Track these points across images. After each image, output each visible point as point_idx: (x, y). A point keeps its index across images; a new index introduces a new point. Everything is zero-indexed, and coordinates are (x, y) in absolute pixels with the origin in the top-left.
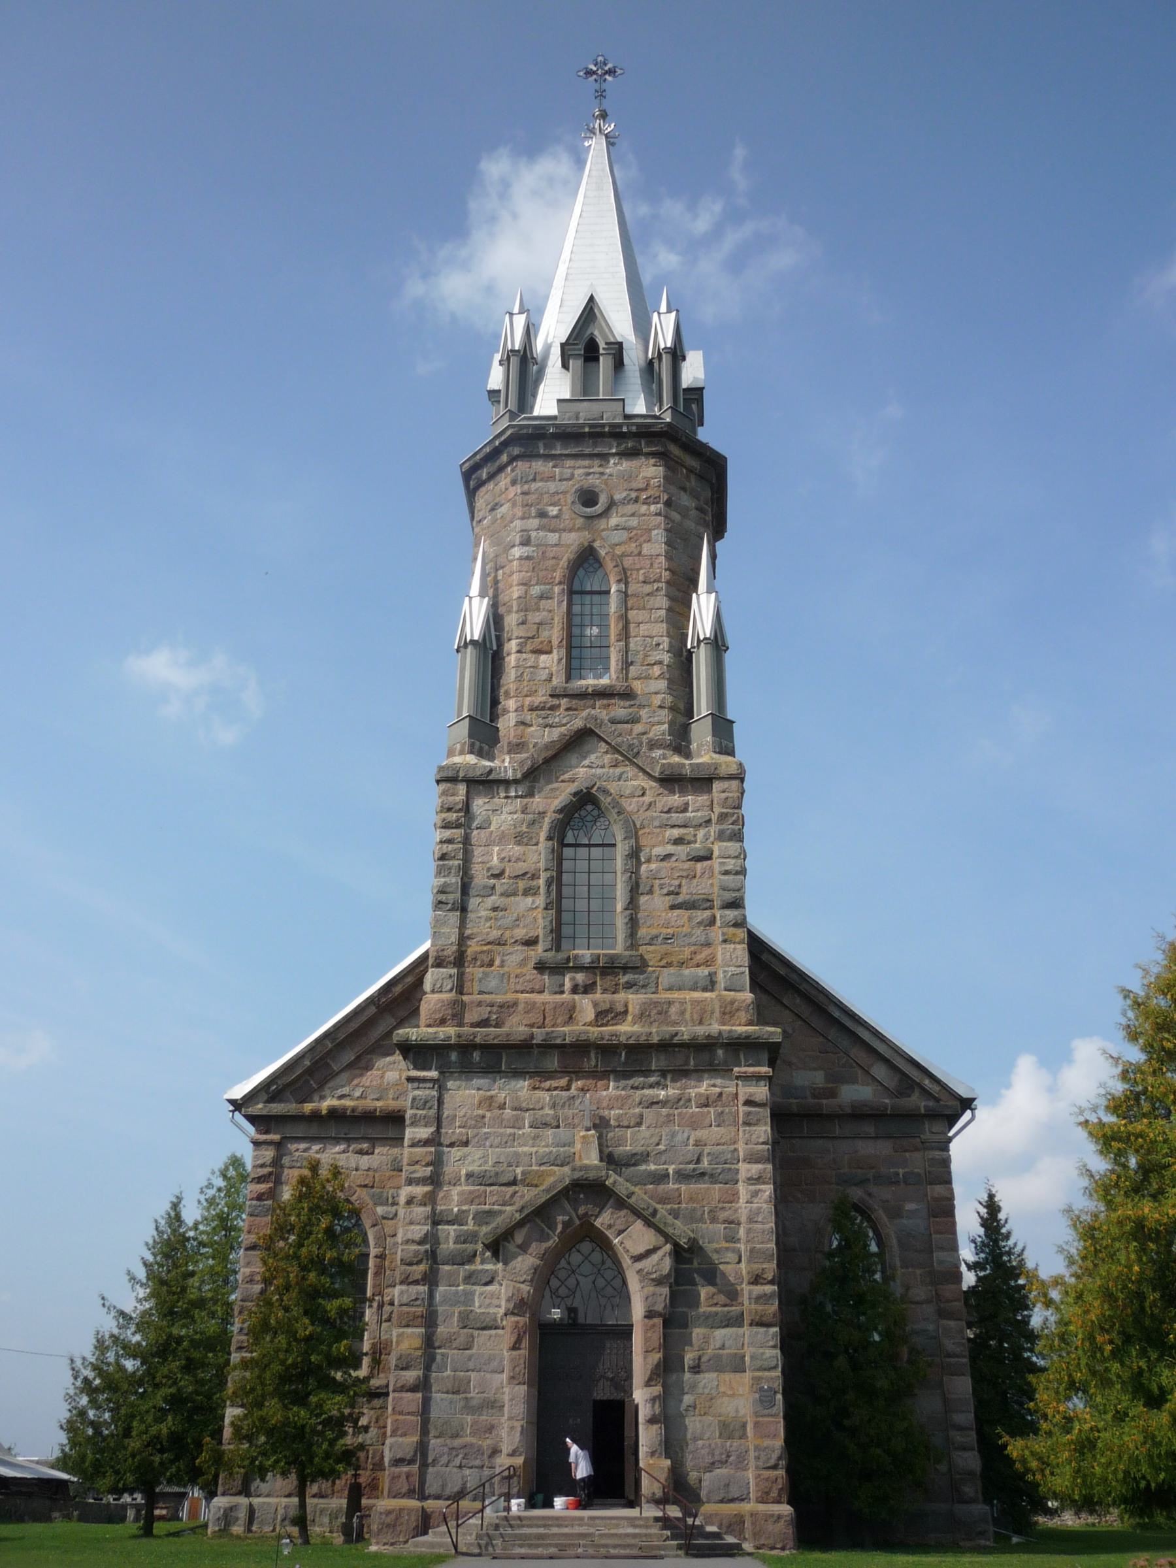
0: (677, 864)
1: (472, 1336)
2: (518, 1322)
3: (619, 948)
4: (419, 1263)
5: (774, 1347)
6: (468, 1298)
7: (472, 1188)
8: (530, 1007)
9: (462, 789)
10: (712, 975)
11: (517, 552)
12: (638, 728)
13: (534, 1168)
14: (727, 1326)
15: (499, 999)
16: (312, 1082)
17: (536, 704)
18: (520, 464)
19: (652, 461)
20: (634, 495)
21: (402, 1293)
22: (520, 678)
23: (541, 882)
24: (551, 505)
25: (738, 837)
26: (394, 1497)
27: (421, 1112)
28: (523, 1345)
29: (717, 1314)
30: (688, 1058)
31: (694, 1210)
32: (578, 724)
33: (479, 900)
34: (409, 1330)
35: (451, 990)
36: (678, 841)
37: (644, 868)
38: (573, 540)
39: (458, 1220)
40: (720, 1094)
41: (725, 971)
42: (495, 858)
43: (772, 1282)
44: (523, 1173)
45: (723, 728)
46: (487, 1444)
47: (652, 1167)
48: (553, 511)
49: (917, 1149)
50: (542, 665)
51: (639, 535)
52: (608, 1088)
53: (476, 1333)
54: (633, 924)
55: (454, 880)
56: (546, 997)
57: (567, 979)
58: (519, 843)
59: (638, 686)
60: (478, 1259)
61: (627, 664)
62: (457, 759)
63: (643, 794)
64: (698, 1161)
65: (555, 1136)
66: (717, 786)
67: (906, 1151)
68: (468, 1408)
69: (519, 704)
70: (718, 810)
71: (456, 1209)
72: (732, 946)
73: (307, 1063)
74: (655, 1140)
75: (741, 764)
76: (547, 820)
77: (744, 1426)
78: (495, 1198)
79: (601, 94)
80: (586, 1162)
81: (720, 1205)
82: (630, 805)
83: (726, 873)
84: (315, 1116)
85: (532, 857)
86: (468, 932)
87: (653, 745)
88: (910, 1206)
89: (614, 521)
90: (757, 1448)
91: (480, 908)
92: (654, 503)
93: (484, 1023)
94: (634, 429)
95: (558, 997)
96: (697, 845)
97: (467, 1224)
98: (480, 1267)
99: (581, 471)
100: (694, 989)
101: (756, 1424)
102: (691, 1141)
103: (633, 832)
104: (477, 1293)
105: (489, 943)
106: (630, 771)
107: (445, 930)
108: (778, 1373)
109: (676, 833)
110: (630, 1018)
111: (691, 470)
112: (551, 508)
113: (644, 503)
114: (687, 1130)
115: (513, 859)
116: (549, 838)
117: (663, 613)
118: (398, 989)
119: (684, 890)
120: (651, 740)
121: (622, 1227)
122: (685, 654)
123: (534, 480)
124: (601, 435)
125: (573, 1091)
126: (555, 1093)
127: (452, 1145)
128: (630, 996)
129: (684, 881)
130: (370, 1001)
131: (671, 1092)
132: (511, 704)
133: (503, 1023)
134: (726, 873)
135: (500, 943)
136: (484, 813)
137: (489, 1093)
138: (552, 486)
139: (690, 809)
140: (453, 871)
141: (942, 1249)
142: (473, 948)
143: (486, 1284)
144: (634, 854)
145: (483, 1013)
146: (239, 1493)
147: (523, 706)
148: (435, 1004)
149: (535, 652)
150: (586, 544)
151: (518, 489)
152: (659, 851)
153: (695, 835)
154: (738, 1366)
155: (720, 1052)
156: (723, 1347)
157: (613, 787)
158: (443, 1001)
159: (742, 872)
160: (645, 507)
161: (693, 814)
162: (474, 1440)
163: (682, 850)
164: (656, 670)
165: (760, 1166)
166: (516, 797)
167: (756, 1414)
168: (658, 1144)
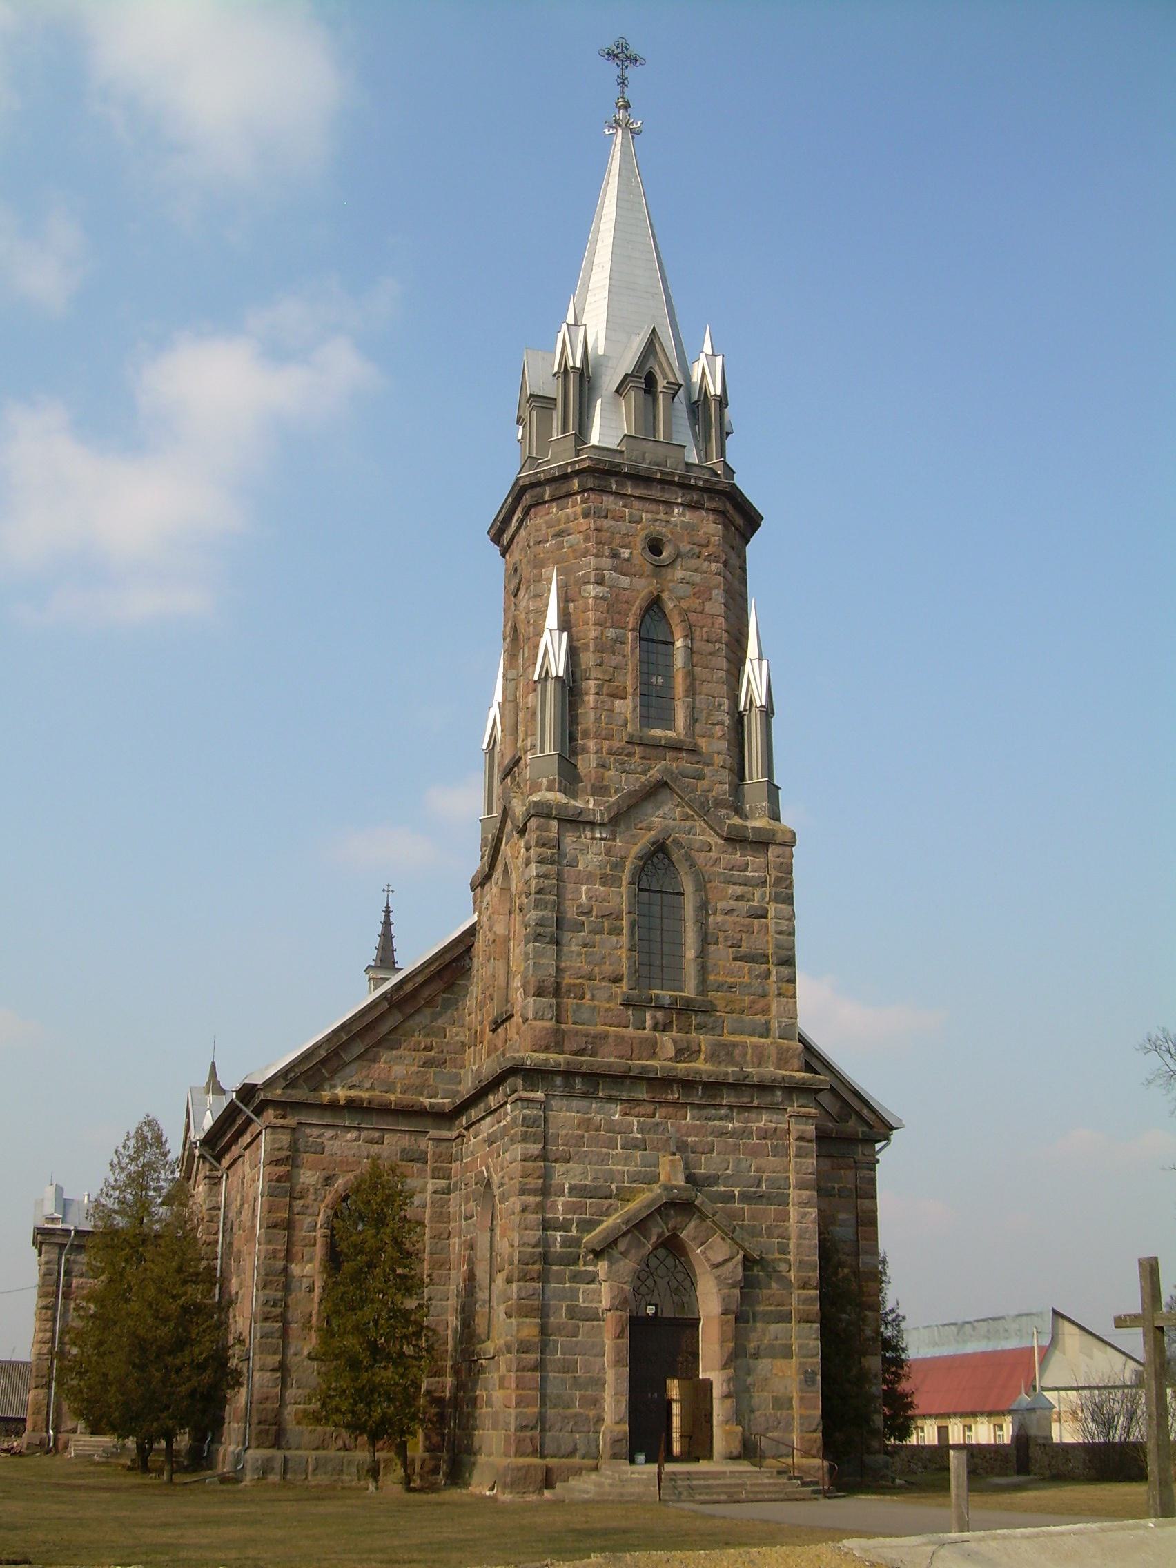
0: (738, 919)
1: (578, 1326)
2: (621, 1316)
3: (690, 991)
4: (534, 1263)
5: (816, 1339)
6: (574, 1293)
7: (574, 1199)
8: (620, 1039)
9: (554, 823)
10: (768, 1023)
11: (592, 590)
12: (704, 784)
13: (626, 1184)
14: (779, 1322)
15: (593, 1030)
16: (323, 1071)
17: (615, 749)
19: (711, 517)
20: (697, 550)
21: (520, 1289)
22: (598, 720)
24: (622, 547)
25: (789, 900)
26: (521, 1456)
27: (531, 1130)
28: (625, 1335)
29: (771, 1311)
30: (752, 1097)
31: (754, 1226)
32: (655, 773)
33: (570, 935)
34: (528, 1320)
35: (552, 1019)
36: (739, 898)
37: (711, 919)
38: (643, 588)
39: (565, 1227)
40: (776, 1129)
41: (779, 1022)
42: (584, 897)
43: (815, 1288)
44: (617, 1188)
45: (773, 791)
46: (592, 1413)
47: (723, 1189)
48: (625, 553)
49: (850, 1168)
50: (617, 710)
51: (703, 593)
52: (686, 1119)
53: (581, 1323)
55: (550, 914)
56: (630, 1031)
57: (648, 1017)
58: (603, 884)
59: (703, 743)
60: (581, 1262)
61: (693, 720)
63: (710, 851)
64: (759, 1186)
65: (642, 1156)
66: (772, 850)
67: (843, 1169)
68: (576, 1384)
69: (599, 746)
70: (774, 873)
71: (561, 1218)
72: (785, 999)
73: (323, 1053)
74: (725, 1165)
75: (794, 834)
76: (628, 866)
77: (791, 1399)
78: (594, 1210)
79: (623, 82)
80: (674, 1183)
81: (775, 1223)
82: (700, 858)
83: (780, 933)
84: (333, 1107)
85: (615, 901)
86: (563, 965)
88: (842, 1216)
89: (679, 573)
90: (802, 1417)
91: (574, 944)
92: (714, 562)
93: (581, 1052)
94: (701, 483)
95: (640, 1031)
96: (755, 904)
97: (571, 1231)
98: (584, 1268)
99: (649, 516)
100: (752, 1034)
101: (802, 1399)
102: (753, 1169)
103: (702, 884)
104: (581, 1290)
105: (580, 977)
106: (700, 824)
107: (544, 961)
108: (818, 1359)
109: (739, 890)
110: (702, 1057)
112: (622, 550)
113: (705, 560)
114: (749, 1158)
115: (600, 899)
116: (631, 883)
117: (723, 674)
118: (409, 987)
119: (744, 944)
120: (716, 799)
121: (704, 1240)
122: (737, 715)
123: (606, 517)
124: (671, 483)
125: (657, 1119)
126: (642, 1119)
127: (556, 1161)
128: (701, 1037)
129: (744, 936)
131: (737, 1125)
132: (592, 745)
133: (597, 1053)
134: (780, 933)
135: (590, 977)
136: (572, 851)
137: (586, 1116)
138: (623, 527)
139: (749, 869)
140: (549, 906)
141: (867, 1253)
142: (567, 980)
143: (588, 1283)
145: (581, 1042)
146: (272, 1446)
147: (602, 749)
148: (540, 1031)
149: (610, 695)
150: (656, 594)
151: (591, 523)
153: (753, 894)
154: (787, 1353)
155: (779, 1093)
156: (776, 1338)
158: (547, 1029)
159: (792, 934)
160: (706, 564)
161: (752, 874)
162: (582, 1411)
163: (744, 906)
164: (718, 731)
165: (808, 1192)
166: (601, 839)
167: (801, 1391)
168: (727, 1169)
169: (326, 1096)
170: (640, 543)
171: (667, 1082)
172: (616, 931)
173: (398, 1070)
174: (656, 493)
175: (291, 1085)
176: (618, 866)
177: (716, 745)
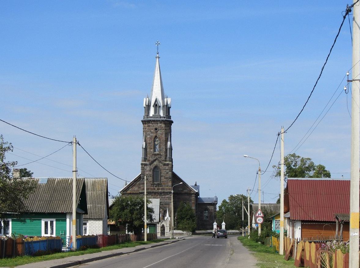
8: (151, 188)
9: (143, 166)
11: (148, 136)
12: (162, 158)
18: (148, 124)
23: (152, 176)
32: (155, 158)
36: (165, 171)
38: (154, 135)
48: (152, 131)
54: (160, 180)
59: (161, 154)
62: (143, 162)
84: (128, 194)
87: (163, 161)
111: (168, 123)
118: (136, 180)
130: (133, 181)
132: (148, 155)
144: (161, 173)
151: (148, 127)
152: (163, 173)
157: (158, 165)
164: (163, 152)
169: (127, 193)
170: (154, 129)
171: (155, 193)
172: (151, 177)
173: (136, 189)
174: (156, 122)
175: (123, 191)
176: (151, 169)
177: (163, 153)
